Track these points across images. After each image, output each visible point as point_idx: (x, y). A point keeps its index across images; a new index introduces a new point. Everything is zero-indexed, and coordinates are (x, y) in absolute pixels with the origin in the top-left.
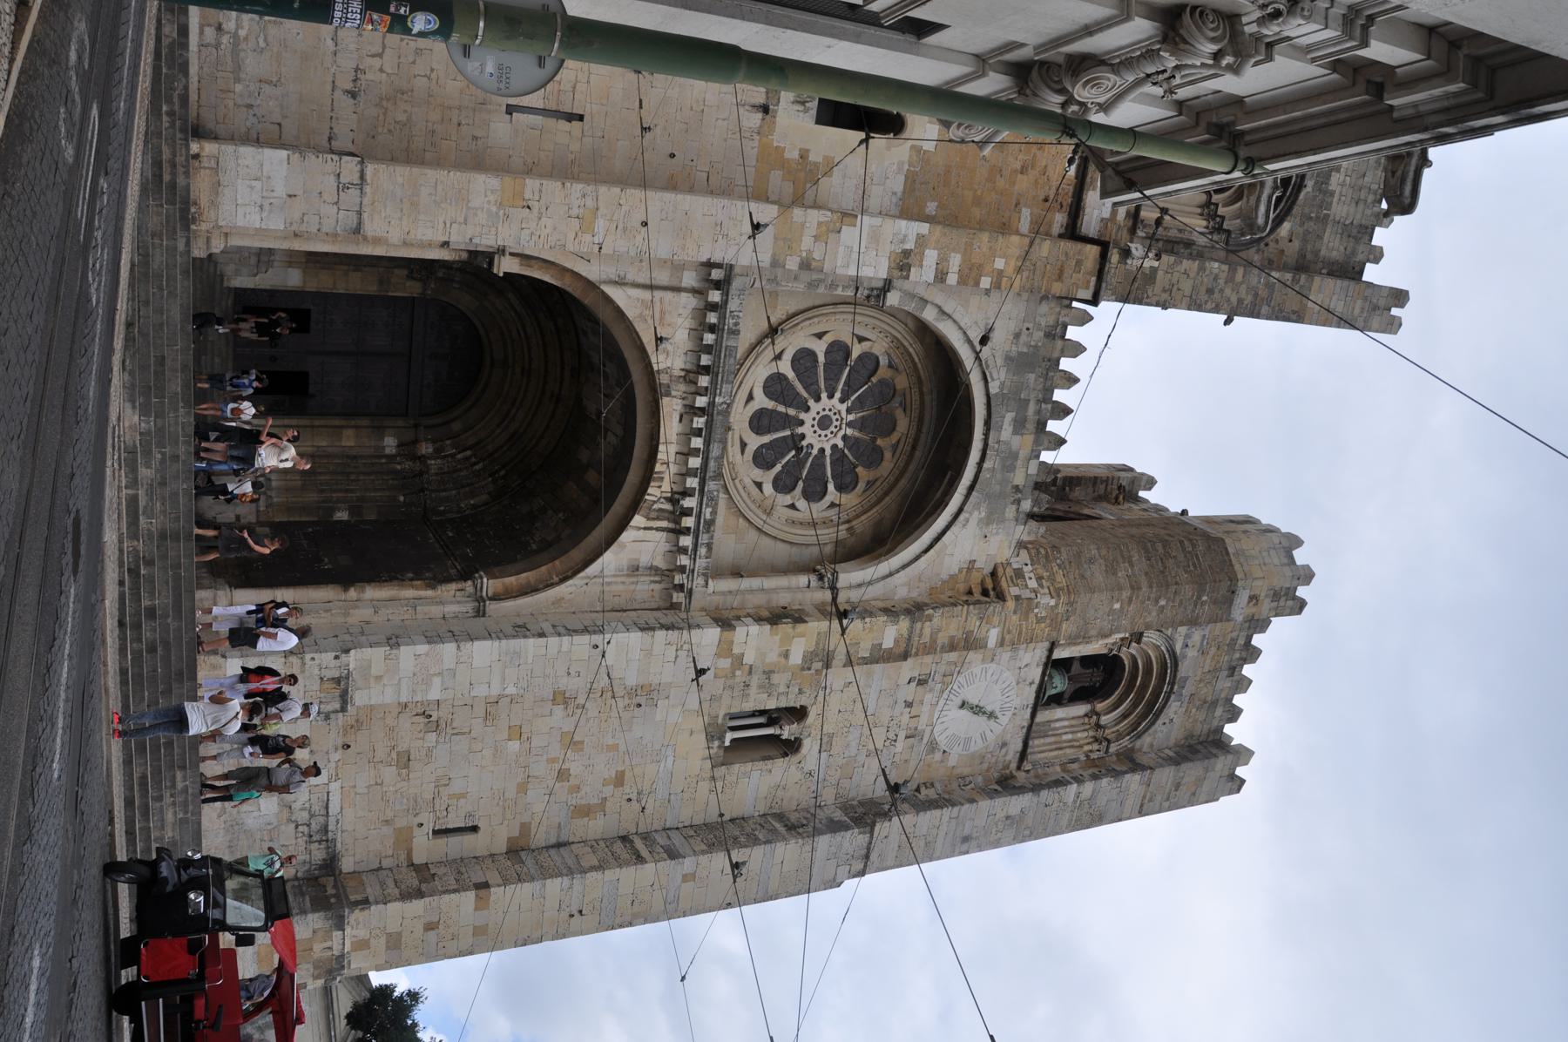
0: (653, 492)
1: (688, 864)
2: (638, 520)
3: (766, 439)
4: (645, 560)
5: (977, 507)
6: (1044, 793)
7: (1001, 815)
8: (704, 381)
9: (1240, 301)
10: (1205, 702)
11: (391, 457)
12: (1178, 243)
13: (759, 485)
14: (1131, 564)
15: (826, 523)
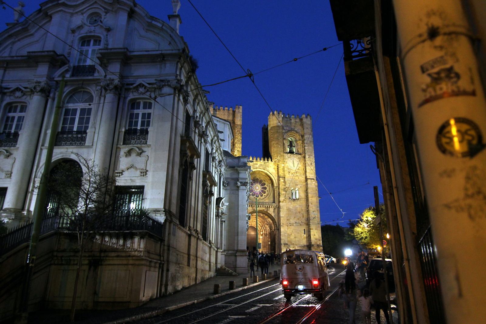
0: (265, 210)
1: (310, 204)
2: (268, 212)
3: (259, 195)
4: (273, 211)
5: (266, 169)
6: (306, 152)
7: (308, 159)
8: (253, 206)
9: (240, 136)
10: (295, 124)
11: (263, 237)
12: (233, 144)
13: (265, 196)
14: (274, 144)
15: (269, 186)
